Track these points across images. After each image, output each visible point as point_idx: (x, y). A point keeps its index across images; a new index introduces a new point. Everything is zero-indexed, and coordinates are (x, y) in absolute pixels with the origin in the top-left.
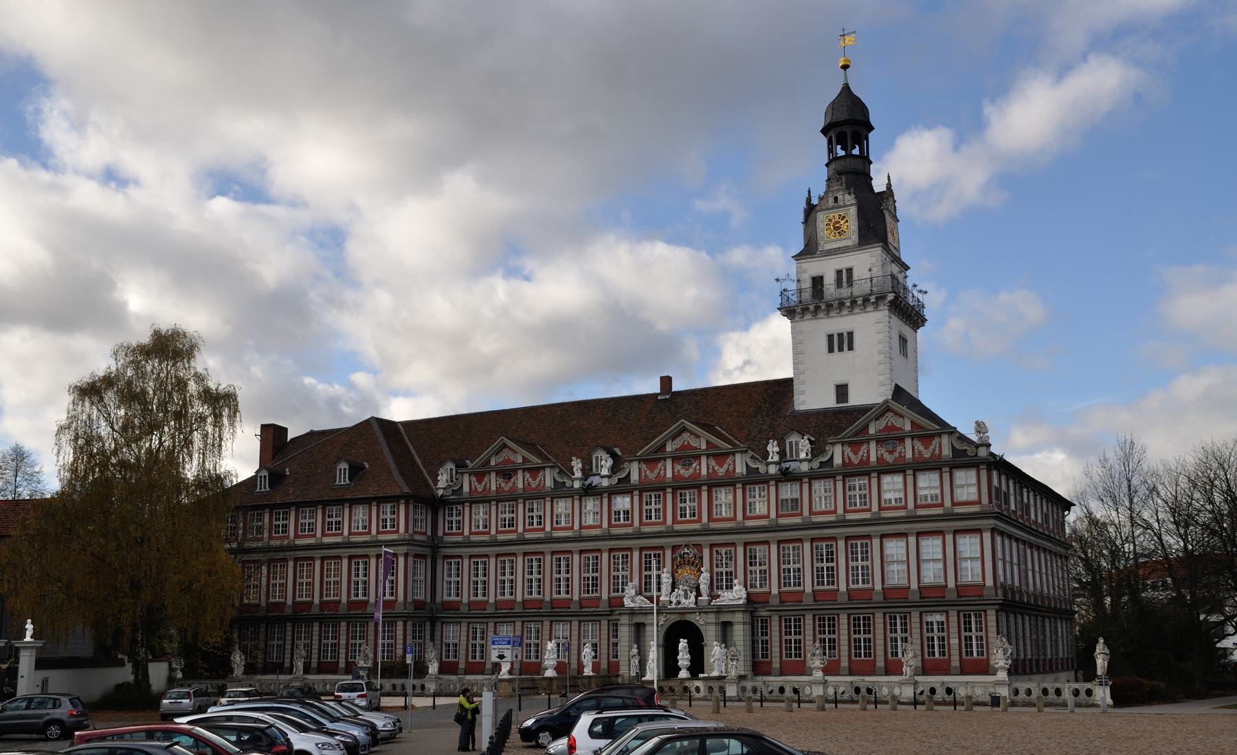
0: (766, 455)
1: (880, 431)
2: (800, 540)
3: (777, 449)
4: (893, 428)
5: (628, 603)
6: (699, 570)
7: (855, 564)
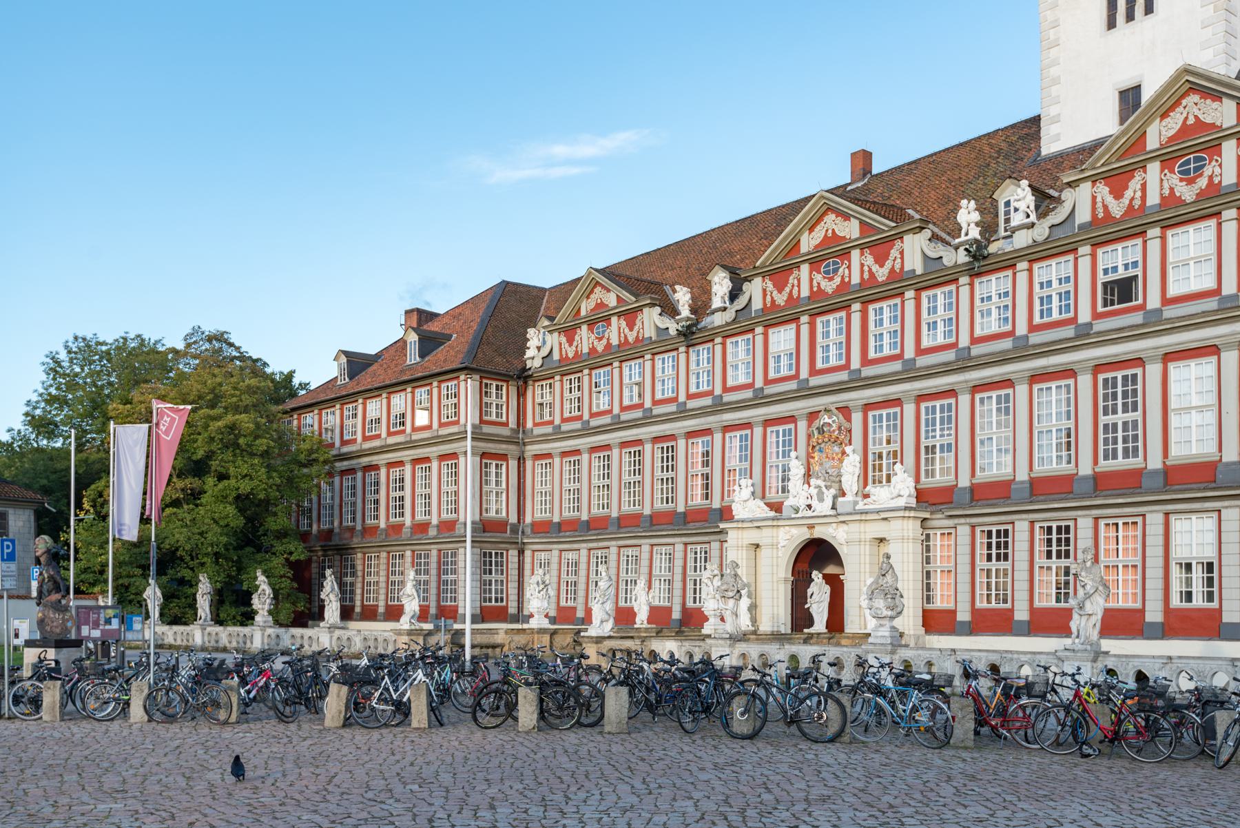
2: (1008, 383)
3: (976, 216)
5: (739, 511)
6: (844, 453)
7: (1110, 419)
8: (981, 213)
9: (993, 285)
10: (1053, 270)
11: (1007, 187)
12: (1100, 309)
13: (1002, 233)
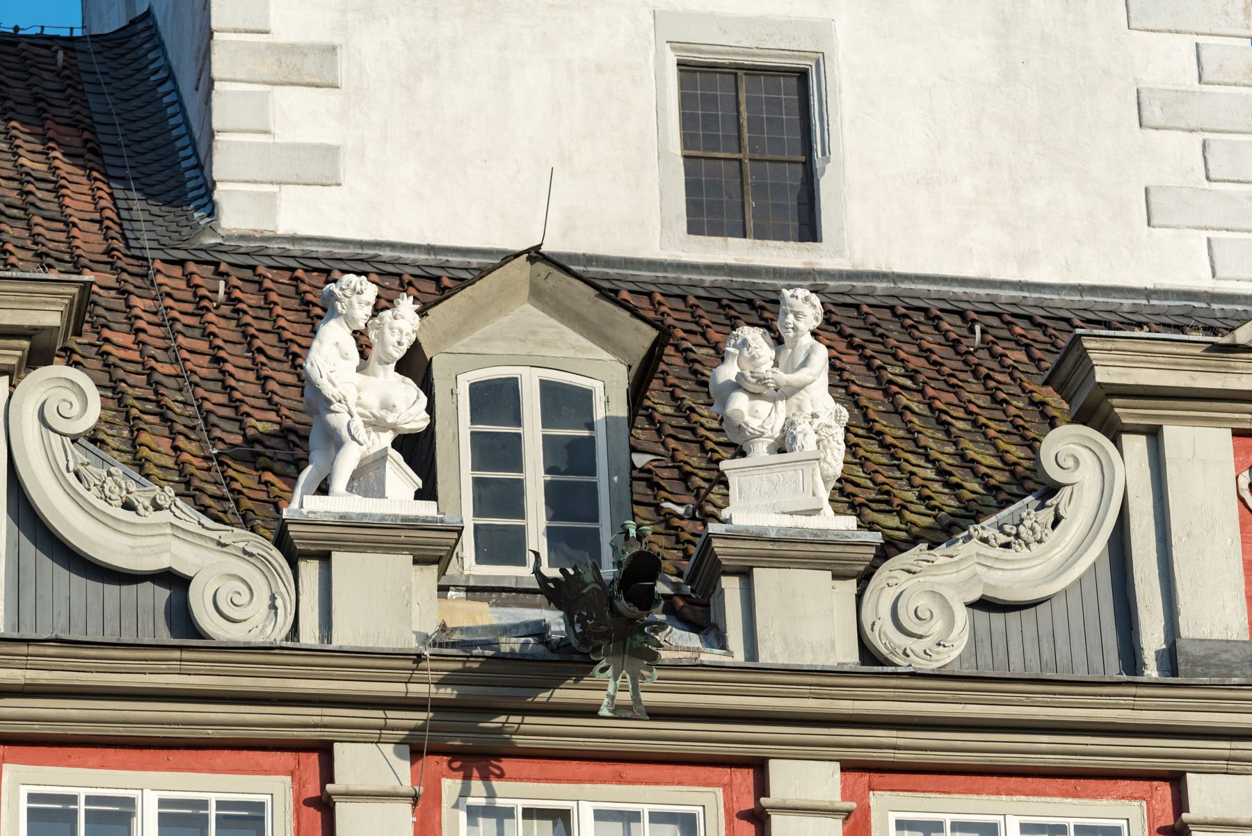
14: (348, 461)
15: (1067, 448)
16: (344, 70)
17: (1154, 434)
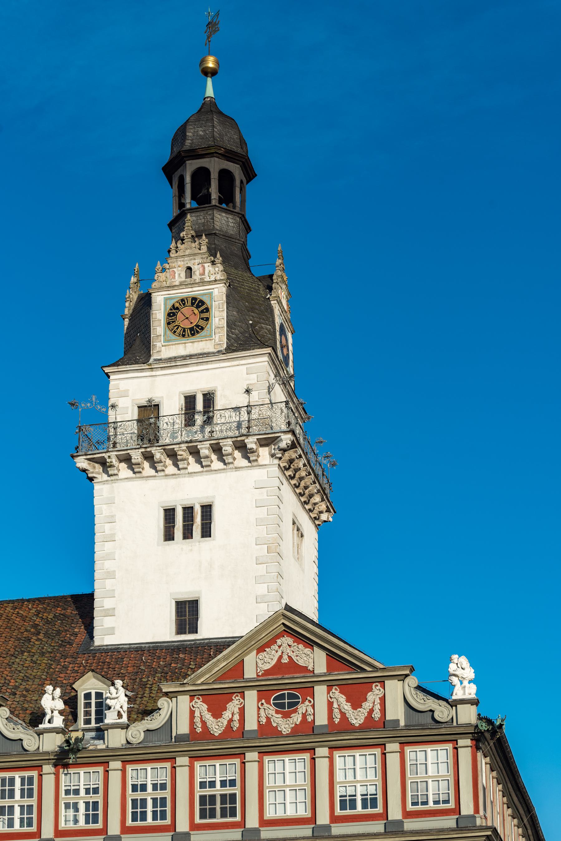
0: (36, 718)
1: (267, 672)
3: (60, 705)
4: (293, 666)
8: (65, 703)
9: (82, 778)
10: (151, 774)
11: (88, 679)
12: (198, 820)
13: (81, 723)
14: (47, 718)
15: (163, 702)
16: (116, 613)
17: (177, 697)
